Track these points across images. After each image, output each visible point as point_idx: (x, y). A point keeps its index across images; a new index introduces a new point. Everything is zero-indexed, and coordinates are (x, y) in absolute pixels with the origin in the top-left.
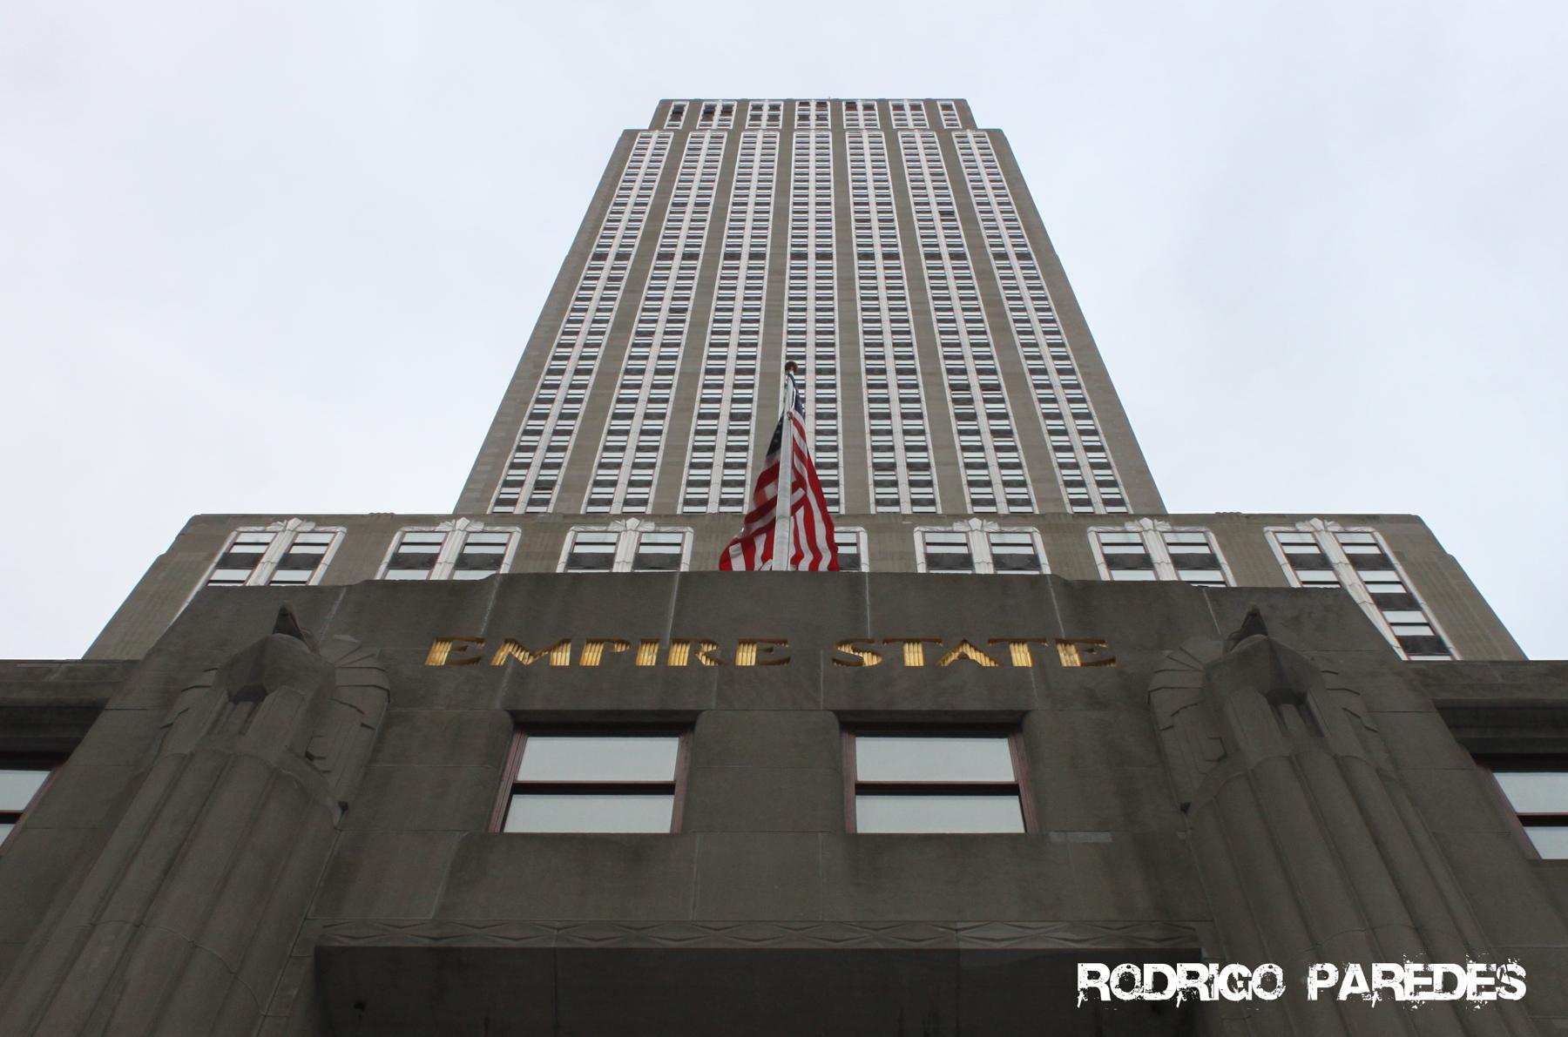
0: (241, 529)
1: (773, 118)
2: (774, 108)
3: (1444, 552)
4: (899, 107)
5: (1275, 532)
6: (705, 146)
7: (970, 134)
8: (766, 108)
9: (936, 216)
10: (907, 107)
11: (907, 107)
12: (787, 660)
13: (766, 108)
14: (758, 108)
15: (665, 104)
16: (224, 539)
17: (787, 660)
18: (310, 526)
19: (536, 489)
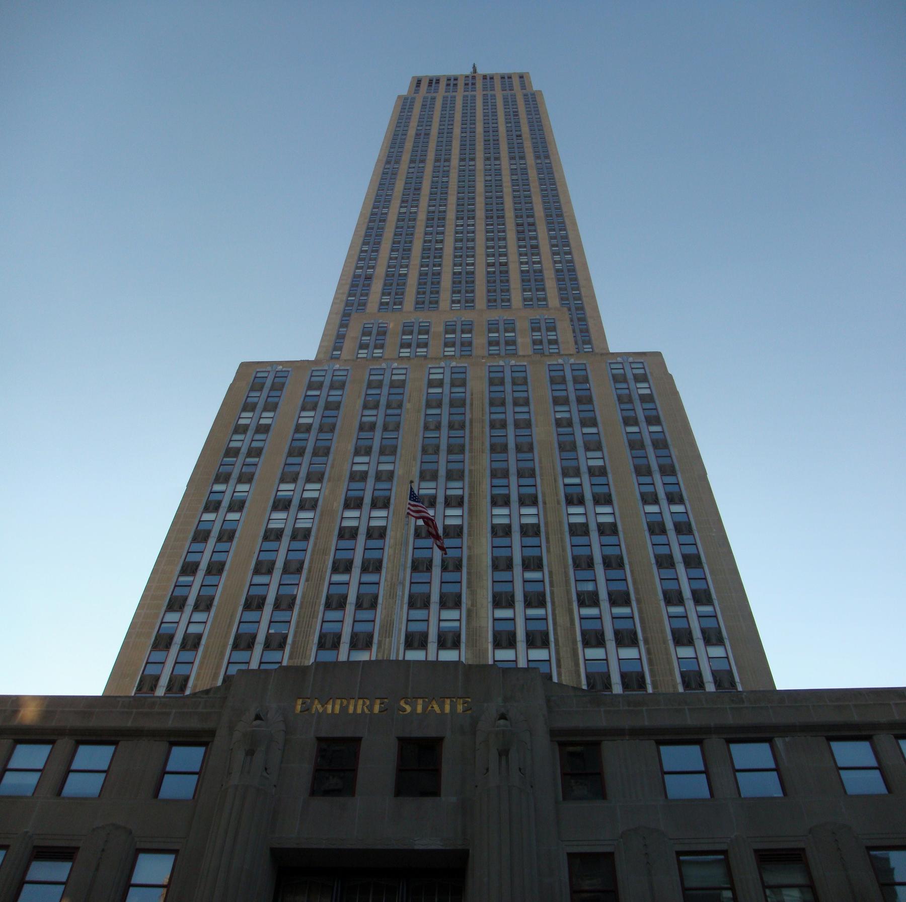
3: (667, 371)
10: (506, 78)
11: (506, 78)
12: (386, 710)
13: (452, 80)
17: (386, 710)
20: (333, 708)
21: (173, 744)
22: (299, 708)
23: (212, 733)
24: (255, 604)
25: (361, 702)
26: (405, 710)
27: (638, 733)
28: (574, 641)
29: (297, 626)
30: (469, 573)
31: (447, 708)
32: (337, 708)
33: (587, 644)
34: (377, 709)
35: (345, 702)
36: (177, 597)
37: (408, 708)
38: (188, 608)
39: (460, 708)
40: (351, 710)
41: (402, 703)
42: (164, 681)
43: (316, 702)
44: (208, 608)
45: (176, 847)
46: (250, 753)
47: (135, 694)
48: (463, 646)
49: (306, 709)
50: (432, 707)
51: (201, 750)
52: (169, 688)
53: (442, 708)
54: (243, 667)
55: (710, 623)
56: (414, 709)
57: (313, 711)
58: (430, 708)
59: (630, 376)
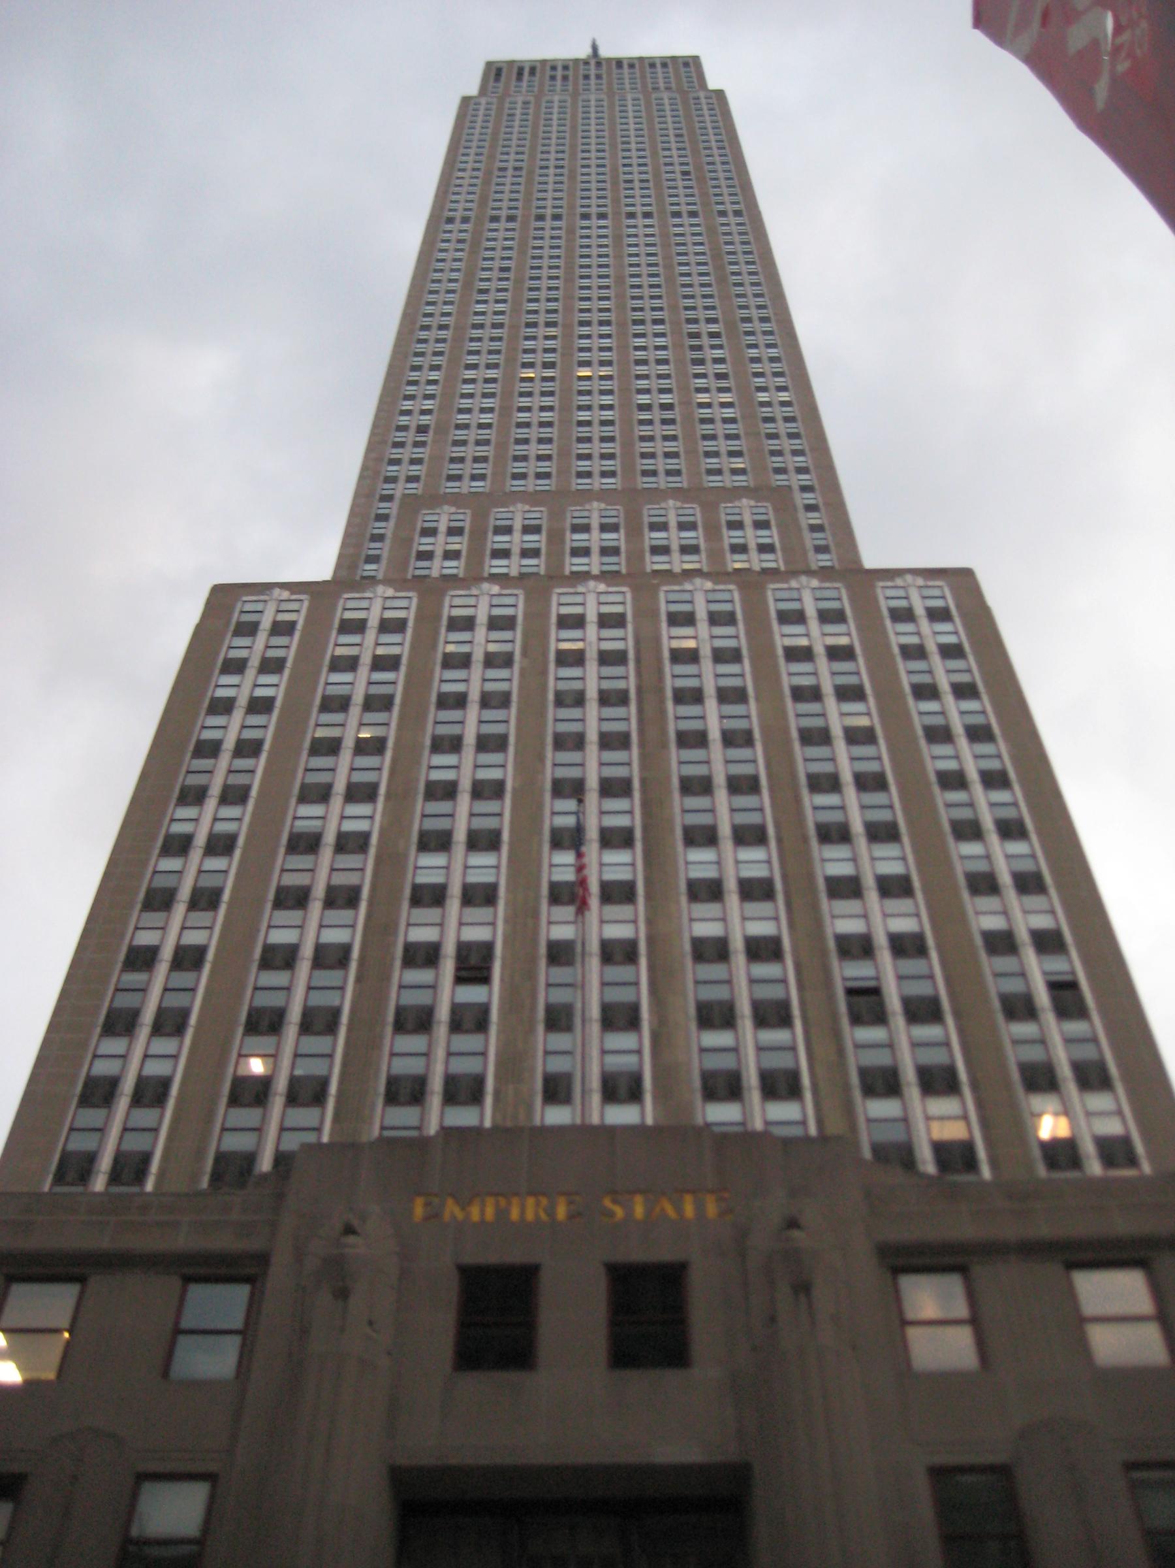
0: (245, 599)
1: (565, 78)
2: (566, 68)
4: (652, 65)
5: (883, 587)
6: (518, 112)
7: (702, 94)
8: (560, 68)
9: (679, 176)
10: (658, 65)
13: (560, 68)
14: (554, 68)
15: (489, 65)
16: (233, 606)
18: (286, 594)
19: (418, 432)
20: (484, 1211)
21: (188, 1280)
22: (419, 1210)
23: (263, 1259)
24: (265, 1023)
25: (531, 1202)
26: (611, 1214)
27: (1031, 1250)
28: (847, 1088)
29: (345, 1064)
30: (651, 968)
31: (689, 1210)
32: (490, 1212)
33: (870, 1091)
34: (561, 1212)
35: (503, 1202)
36: (120, 1010)
37: (619, 1212)
38: (144, 1032)
39: (712, 1209)
40: (515, 1214)
41: (607, 1202)
42: (105, 1163)
43: (450, 1202)
44: (179, 1030)
45: (212, 1467)
46: (343, 1294)
47: (51, 1189)
48: (648, 1098)
49: (433, 1216)
50: (663, 1210)
51: (242, 1292)
52: (115, 1177)
53: (679, 1210)
54: (311, 1138)
55: (1087, 1053)
56: (629, 1211)
57: (447, 1216)
58: (657, 1210)
59: (919, 611)
